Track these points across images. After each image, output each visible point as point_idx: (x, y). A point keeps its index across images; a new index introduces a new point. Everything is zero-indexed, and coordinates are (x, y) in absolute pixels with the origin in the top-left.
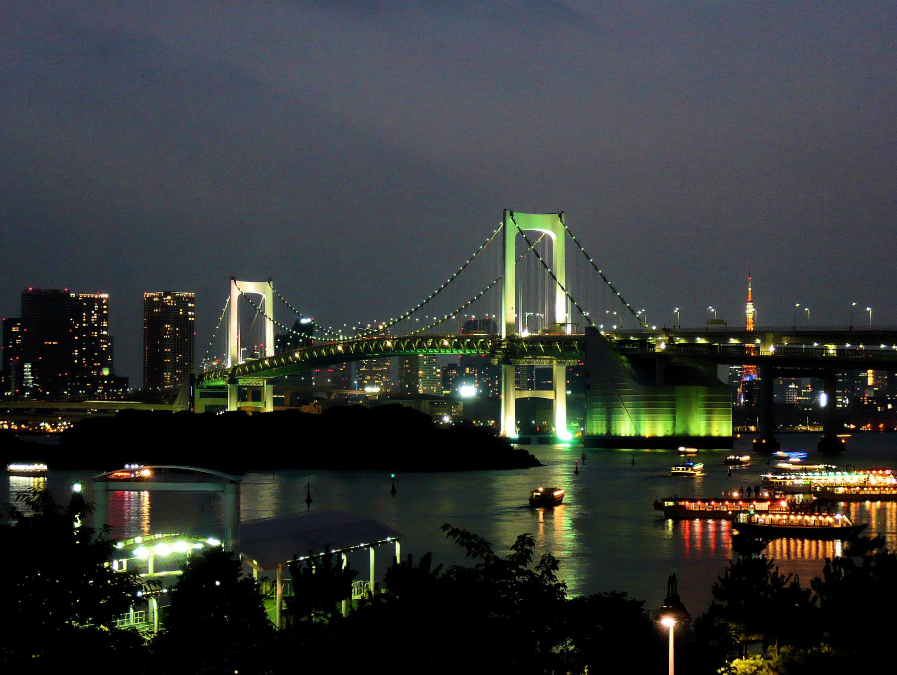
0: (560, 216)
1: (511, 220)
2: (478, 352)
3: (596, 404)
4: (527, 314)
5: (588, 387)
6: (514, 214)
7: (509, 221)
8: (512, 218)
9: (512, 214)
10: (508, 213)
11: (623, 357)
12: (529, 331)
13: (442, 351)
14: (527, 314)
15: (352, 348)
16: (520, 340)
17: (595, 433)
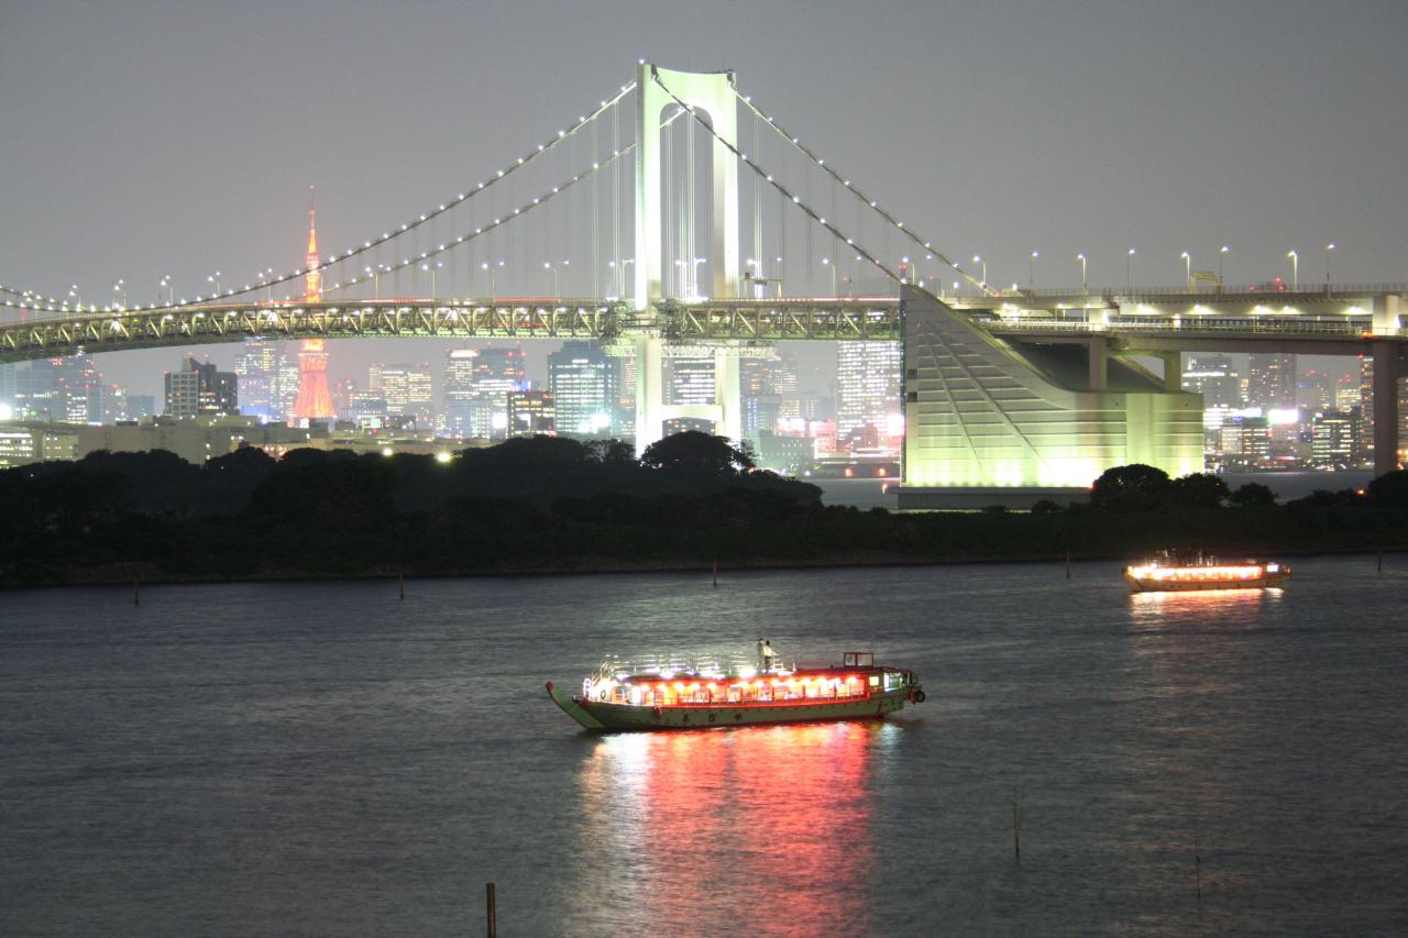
0: (730, 78)
1: (654, 82)
2: (552, 334)
3: (935, 429)
4: (696, 262)
5: (913, 397)
6: (659, 70)
7: (650, 85)
8: (656, 79)
9: (654, 71)
10: (648, 69)
11: (999, 342)
12: (702, 292)
13: (443, 332)
14: (696, 262)
15: (158, 325)
16: (685, 308)
17: (932, 483)
